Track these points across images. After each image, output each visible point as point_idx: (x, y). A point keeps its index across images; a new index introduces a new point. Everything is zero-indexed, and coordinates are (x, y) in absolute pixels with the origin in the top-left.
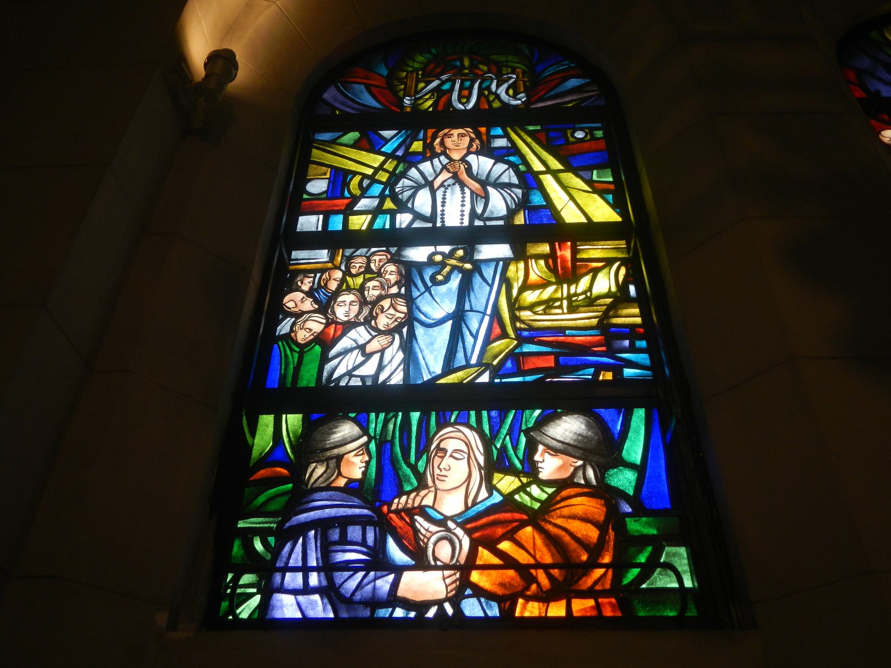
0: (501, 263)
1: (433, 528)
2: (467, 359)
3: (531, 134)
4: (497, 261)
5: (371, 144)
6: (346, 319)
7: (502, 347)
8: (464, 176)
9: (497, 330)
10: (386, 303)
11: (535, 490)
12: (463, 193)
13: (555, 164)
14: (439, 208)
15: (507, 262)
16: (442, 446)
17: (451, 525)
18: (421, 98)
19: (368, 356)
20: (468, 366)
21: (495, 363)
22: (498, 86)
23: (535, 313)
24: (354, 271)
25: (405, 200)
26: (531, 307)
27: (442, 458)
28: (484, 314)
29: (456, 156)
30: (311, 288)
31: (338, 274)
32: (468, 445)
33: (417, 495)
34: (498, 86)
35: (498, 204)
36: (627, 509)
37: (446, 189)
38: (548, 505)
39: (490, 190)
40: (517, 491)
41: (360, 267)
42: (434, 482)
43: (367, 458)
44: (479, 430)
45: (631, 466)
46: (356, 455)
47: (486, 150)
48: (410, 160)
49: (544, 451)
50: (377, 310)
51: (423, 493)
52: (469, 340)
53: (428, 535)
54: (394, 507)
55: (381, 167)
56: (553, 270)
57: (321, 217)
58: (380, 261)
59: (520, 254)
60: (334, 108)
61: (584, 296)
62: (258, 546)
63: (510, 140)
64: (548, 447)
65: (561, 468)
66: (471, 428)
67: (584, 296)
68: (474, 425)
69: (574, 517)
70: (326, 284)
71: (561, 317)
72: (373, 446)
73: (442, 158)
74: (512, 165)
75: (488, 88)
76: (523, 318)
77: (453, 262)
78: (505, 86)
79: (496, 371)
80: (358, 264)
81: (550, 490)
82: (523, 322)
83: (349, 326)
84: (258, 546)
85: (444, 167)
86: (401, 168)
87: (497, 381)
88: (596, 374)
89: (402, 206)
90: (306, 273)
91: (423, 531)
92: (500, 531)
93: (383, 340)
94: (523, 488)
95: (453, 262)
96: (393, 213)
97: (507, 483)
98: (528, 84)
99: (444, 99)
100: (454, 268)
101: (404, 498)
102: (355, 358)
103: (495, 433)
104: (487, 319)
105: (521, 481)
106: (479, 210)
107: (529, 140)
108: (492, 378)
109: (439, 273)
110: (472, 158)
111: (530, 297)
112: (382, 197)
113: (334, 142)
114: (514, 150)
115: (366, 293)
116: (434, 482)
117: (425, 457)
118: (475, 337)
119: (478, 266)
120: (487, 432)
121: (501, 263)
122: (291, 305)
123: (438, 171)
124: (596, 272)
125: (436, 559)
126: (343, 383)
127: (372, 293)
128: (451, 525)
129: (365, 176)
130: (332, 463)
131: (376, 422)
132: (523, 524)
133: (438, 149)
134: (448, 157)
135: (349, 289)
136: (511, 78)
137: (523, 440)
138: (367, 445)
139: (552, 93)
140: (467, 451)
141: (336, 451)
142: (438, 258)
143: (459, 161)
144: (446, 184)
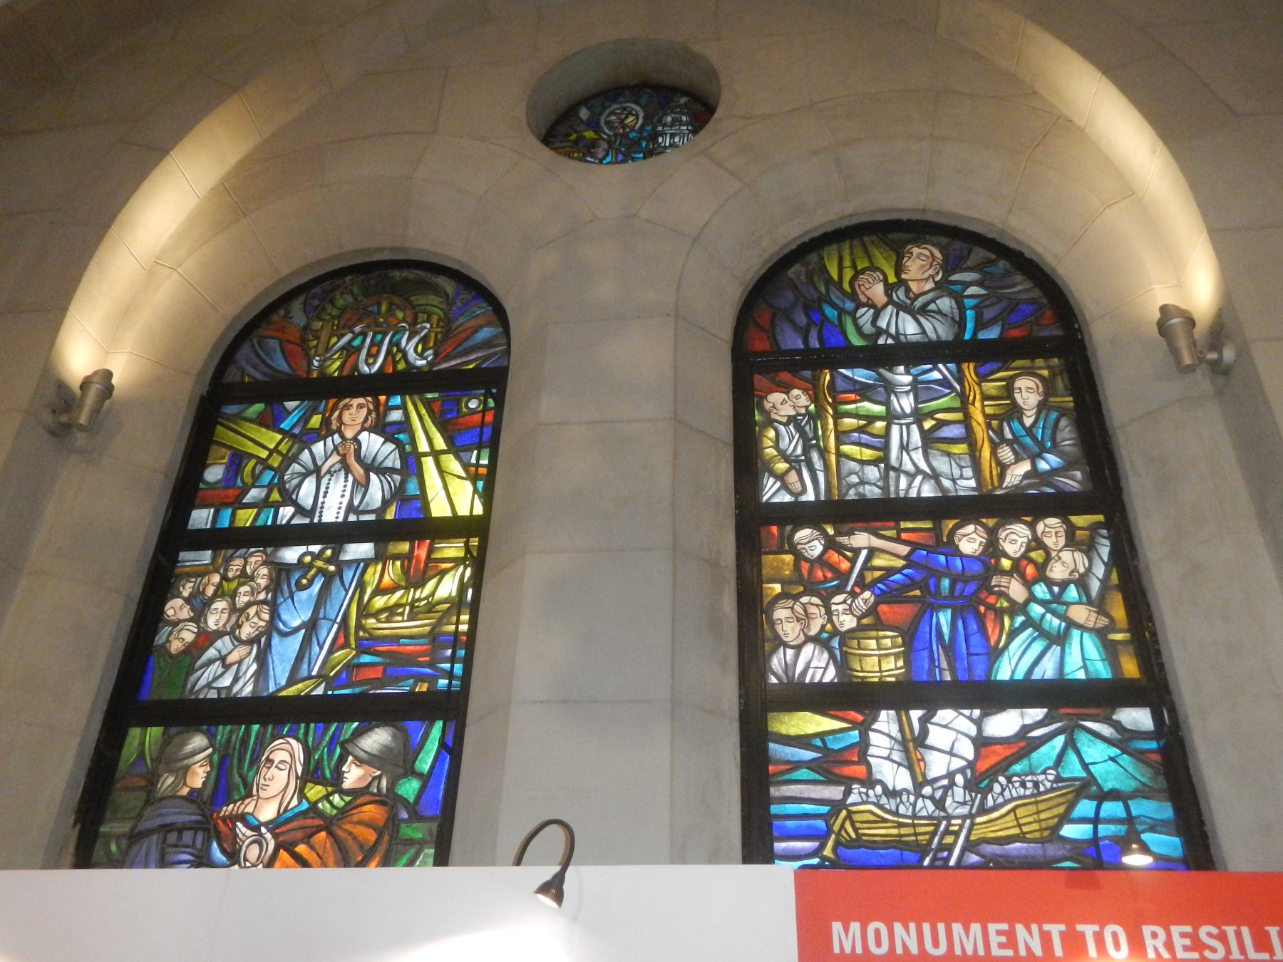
0: (362, 564)
1: (249, 833)
2: (310, 670)
3: (428, 405)
4: (358, 561)
5: (270, 421)
6: (215, 628)
7: (342, 657)
8: (352, 460)
9: (341, 640)
10: (252, 611)
11: (336, 799)
12: (346, 477)
13: (440, 443)
14: (321, 499)
15: (367, 563)
16: (271, 757)
17: (263, 830)
18: (330, 358)
19: (226, 667)
20: (310, 677)
21: (332, 674)
22: (409, 339)
23: (379, 621)
24: (230, 575)
25: (291, 490)
26: (376, 615)
27: (269, 768)
28: (335, 621)
29: (349, 434)
30: (191, 594)
31: (216, 578)
32: (292, 756)
33: (242, 803)
34: (409, 339)
35: (376, 491)
36: (404, 815)
37: (332, 475)
38: (344, 812)
39: (373, 476)
40: (320, 800)
41: (237, 570)
42: (258, 791)
43: (209, 769)
44: (304, 744)
45: (419, 775)
46: (201, 766)
47: (381, 428)
48: (305, 438)
49: (352, 762)
50: (243, 618)
51: (247, 801)
52: (316, 648)
53: (244, 838)
54: (222, 814)
55: (275, 450)
56: (405, 571)
57: (212, 510)
58: (256, 563)
59: (381, 557)
60: (243, 373)
61: (425, 602)
62: (114, 848)
63: (407, 415)
64: (356, 758)
65: (361, 778)
66: (298, 740)
67: (425, 602)
68: (301, 736)
69: (361, 823)
70: (204, 589)
71: (401, 625)
72: (216, 757)
73: (336, 436)
74: (399, 445)
75: (398, 344)
76: (368, 626)
77: (320, 563)
78: (416, 339)
79: (331, 683)
80: (236, 565)
81: (348, 799)
82: (365, 630)
83: (219, 634)
84: (114, 848)
85: (336, 448)
86: (294, 450)
87: (330, 693)
88: (415, 685)
89: (289, 498)
90: (189, 576)
91: (240, 835)
92: (299, 834)
93: (242, 650)
94: (327, 797)
95: (320, 563)
96: (277, 506)
97: (315, 792)
98: (439, 336)
99: (351, 361)
100: (321, 571)
101: (232, 805)
102: (216, 668)
103: (316, 747)
104: (336, 626)
105: (327, 790)
106: (356, 503)
107: (423, 411)
108: (326, 689)
109: (304, 577)
110: (364, 436)
111: (379, 602)
112: (270, 487)
113: (239, 417)
114: (405, 426)
115: (237, 598)
116: (258, 791)
117: (255, 768)
118: (321, 648)
119: (341, 566)
120: (310, 743)
121: (362, 564)
122: (170, 612)
123: (329, 453)
124: (443, 573)
125: (246, 860)
126: (201, 696)
127: (242, 600)
128: (263, 830)
129: (260, 461)
130: (180, 776)
131: (222, 731)
132: (319, 829)
133: (334, 427)
134: (342, 436)
135: (223, 596)
136: (425, 328)
137: (338, 750)
138: (210, 756)
139: (460, 349)
140: (290, 762)
141: (186, 762)
142: (308, 559)
143: (351, 440)
144: (333, 470)
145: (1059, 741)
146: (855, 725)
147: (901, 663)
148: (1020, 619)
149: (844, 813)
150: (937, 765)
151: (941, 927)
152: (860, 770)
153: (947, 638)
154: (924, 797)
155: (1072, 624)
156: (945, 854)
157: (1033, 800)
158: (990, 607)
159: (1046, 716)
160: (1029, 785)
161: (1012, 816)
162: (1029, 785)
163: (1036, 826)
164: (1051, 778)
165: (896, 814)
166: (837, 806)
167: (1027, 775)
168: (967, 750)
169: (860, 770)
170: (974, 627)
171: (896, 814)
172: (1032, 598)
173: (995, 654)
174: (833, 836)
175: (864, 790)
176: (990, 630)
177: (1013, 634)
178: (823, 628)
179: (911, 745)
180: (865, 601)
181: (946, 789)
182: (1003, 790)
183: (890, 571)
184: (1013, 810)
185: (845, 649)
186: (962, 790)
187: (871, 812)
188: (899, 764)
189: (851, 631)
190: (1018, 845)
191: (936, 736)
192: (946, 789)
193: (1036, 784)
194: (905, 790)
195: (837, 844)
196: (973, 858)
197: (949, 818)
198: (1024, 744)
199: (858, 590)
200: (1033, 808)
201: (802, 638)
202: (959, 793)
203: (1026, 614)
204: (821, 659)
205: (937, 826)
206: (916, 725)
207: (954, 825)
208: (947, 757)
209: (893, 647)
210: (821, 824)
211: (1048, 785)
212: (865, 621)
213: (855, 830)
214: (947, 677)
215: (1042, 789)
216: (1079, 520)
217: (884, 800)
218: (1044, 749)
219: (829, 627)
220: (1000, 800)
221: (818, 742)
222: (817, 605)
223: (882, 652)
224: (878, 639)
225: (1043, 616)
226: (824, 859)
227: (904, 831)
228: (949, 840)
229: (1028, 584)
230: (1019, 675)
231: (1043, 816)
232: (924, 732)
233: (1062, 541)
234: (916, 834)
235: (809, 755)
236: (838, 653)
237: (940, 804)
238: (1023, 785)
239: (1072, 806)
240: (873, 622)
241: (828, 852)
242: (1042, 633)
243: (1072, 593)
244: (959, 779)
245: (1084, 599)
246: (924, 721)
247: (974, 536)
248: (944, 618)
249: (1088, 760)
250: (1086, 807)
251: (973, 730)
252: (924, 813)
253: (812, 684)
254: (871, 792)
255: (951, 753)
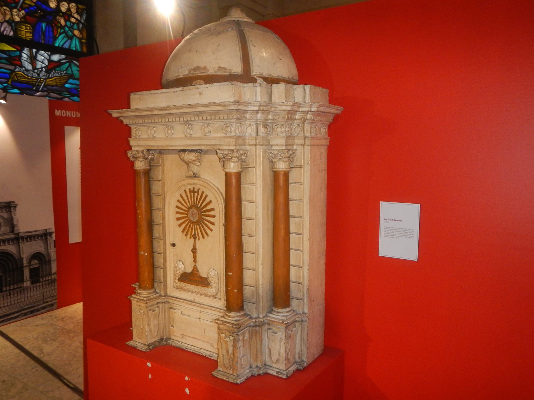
145: (67, 64)
146: (18, 50)
147: (31, 35)
148: (62, 30)
149: (14, 74)
150: (39, 65)
151: (75, 112)
152: (19, 62)
153: (44, 31)
154: (35, 72)
155: (74, 35)
156: (39, 87)
157: (60, 77)
158: (56, 25)
159: (65, 57)
160: (60, 74)
161: (55, 80)
162: (60, 74)
163: (60, 83)
164: (65, 73)
165: (27, 75)
166: (13, 71)
167: (59, 71)
168: (46, 62)
169: (19, 62)
170: (51, 29)
171: (27, 75)
172: (66, 25)
173: (55, 39)
174: (11, 79)
175: (20, 68)
176: (55, 31)
177: (60, 34)
178: (10, 18)
179: (33, 59)
180: (23, 13)
181: (41, 71)
182: (54, 74)
183: (30, 5)
184: (55, 79)
185: (16, 27)
186: (44, 72)
187: (21, 74)
188: (29, 63)
189: (18, 22)
190: (55, 87)
191: (40, 58)
192: (41, 71)
193: (61, 74)
194: (30, 70)
195: (12, 81)
196: (45, 89)
197: (41, 79)
198: (59, 64)
199: (21, 9)
200: (60, 79)
201: (3, 20)
202: (43, 73)
203: (64, 29)
204: (8, 29)
205: (38, 80)
206: (34, 53)
207: (42, 80)
208: (41, 63)
209: (30, 30)
210: (8, 75)
211: (64, 74)
212: (22, 20)
213: (17, 78)
214: (43, 42)
215: (62, 75)
216: (80, 6)
217: (25, 72)
218: (64, 66)
219: (11, 19)
220: (53, 76)
221: (8, 53)
222: (8, 11)
223: (26, 30)
224: (26, 26)
225: (68, 31)
226: (9, 84)
227: (29, 80)
228: (40, 84)
229: (66, 21)
230: (60, 46)
231: (62, 81)
232: (36, 56)
233: (75, 11)
234: (33, 81)
235: (5, 56)
236: (14, 28)
237: (39, 75)
238: (58, 73)
239: (68, 80)
240: (24, 21)
241: (9, 83)
242: (67, 36)
243: (75, 26)
244: (44, 69)
245: (78, 29)
246: (37, 52)
247: (54, 2)
248: (44, 25)
249: (73, 70)
250: (71, 81)
251: (48, 58)
252: (35, 77)
253: (6, 35)
254: (22, 69)
255: (43, 63)
